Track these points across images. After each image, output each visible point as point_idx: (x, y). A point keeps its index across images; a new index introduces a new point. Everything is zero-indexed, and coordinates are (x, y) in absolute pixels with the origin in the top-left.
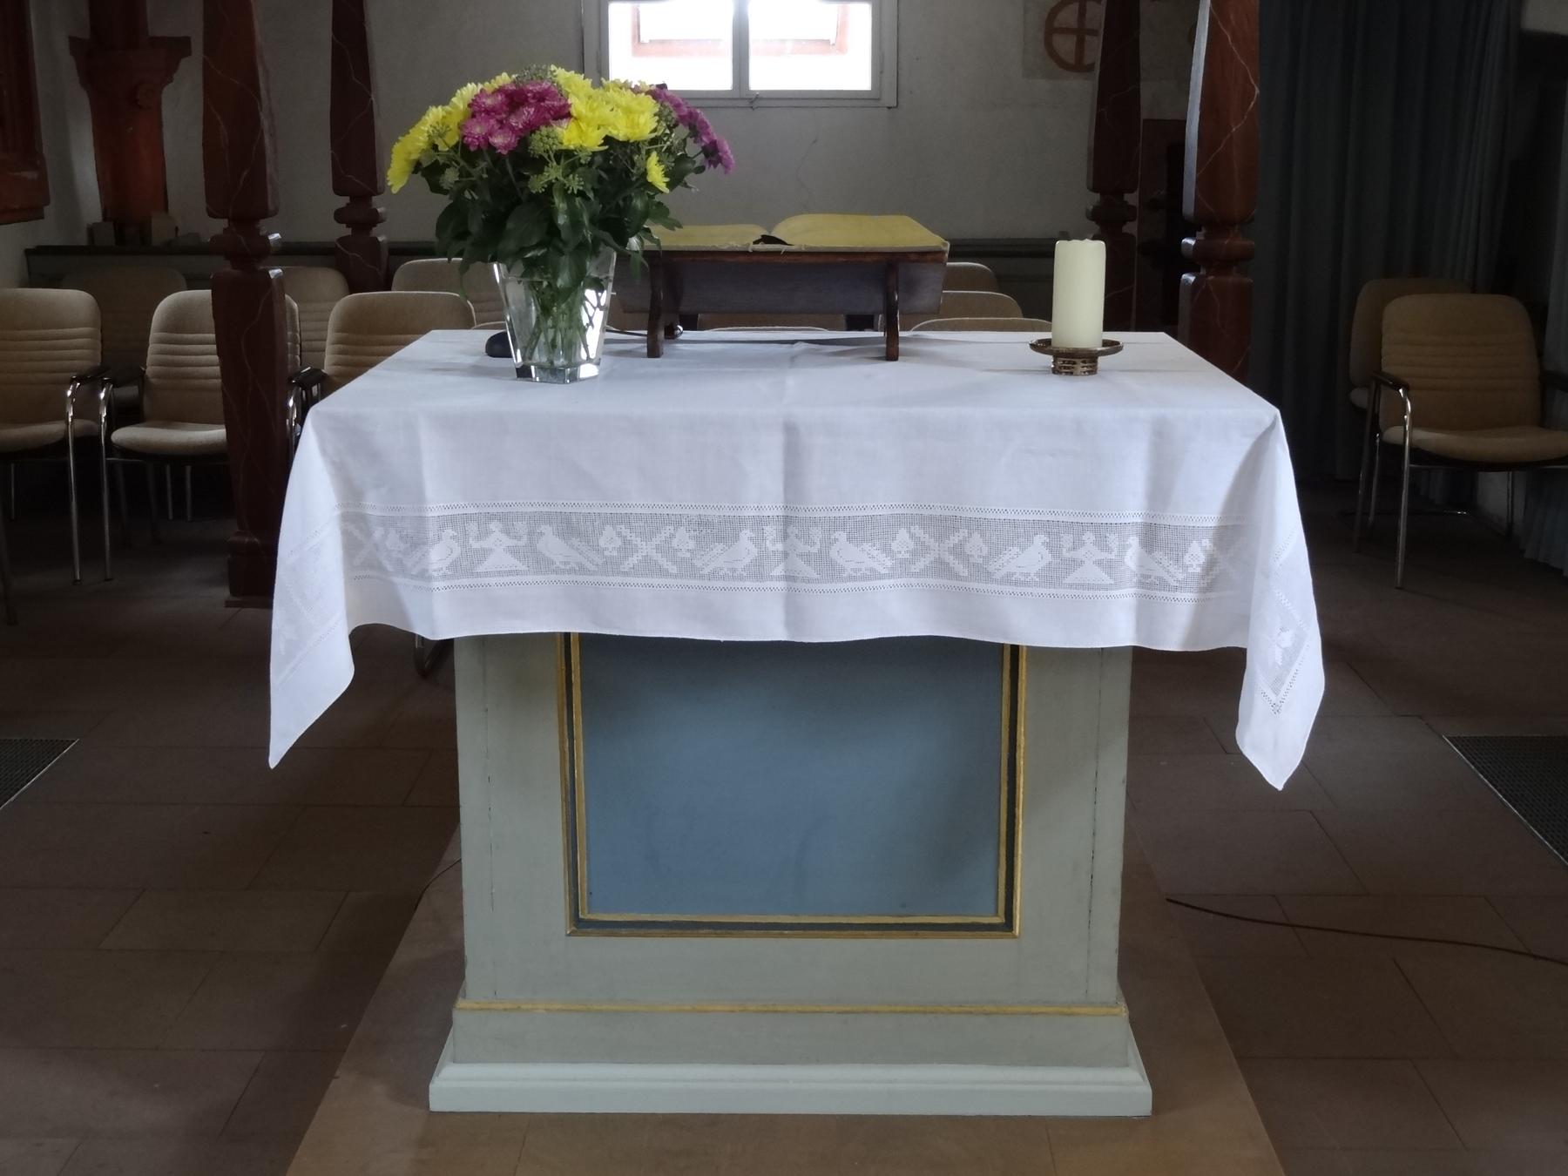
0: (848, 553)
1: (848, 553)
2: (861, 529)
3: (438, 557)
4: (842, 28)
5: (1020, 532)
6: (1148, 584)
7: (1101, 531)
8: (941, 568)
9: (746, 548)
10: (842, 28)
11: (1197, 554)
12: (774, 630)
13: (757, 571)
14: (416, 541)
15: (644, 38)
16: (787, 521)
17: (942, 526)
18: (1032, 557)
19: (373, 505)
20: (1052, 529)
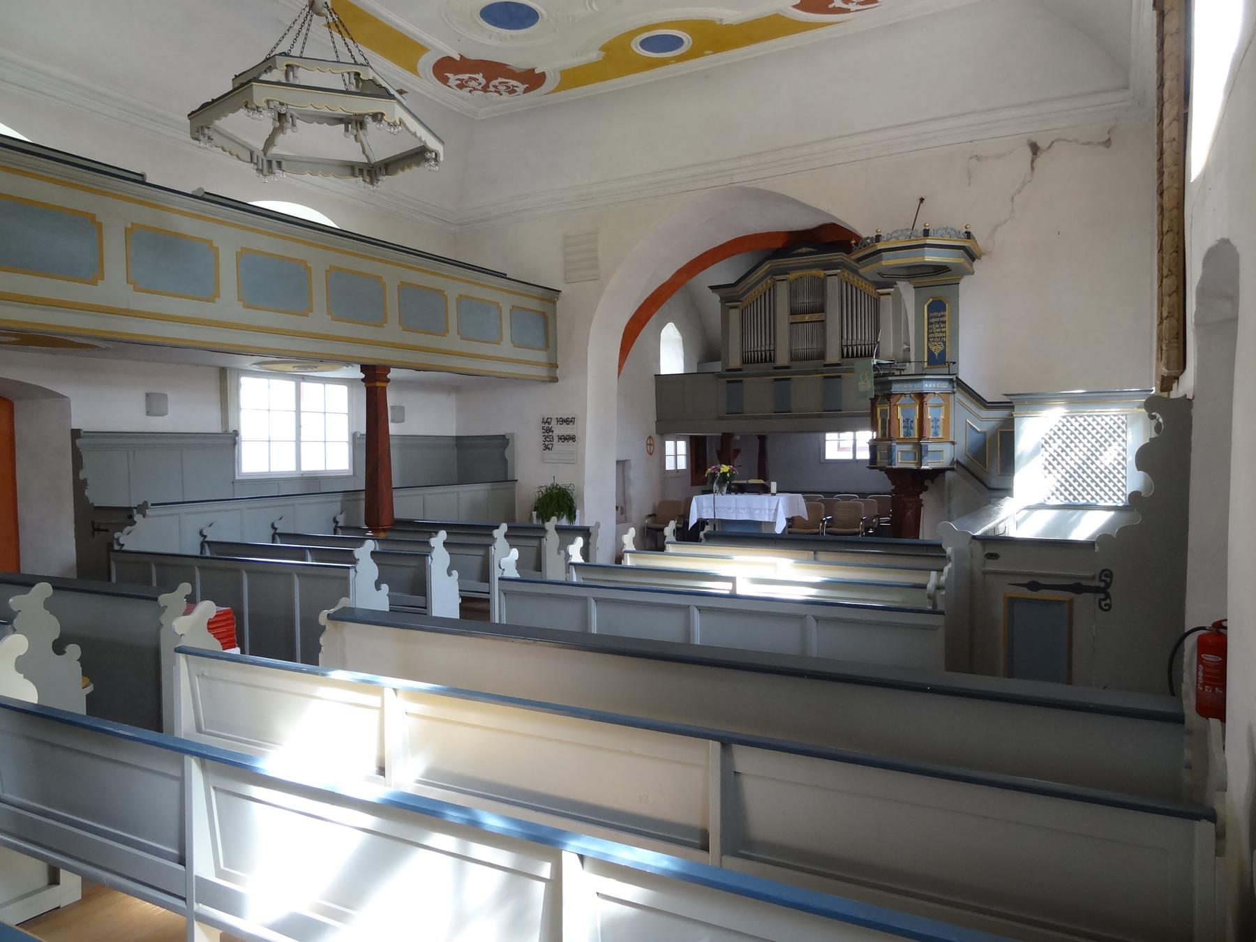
0: (741, 511)
1: (741, 511)
2: (742, 509)
3: (704, 510)
4: (844, 449)
5: (756, 509)
6: (769, 514)
7: (764, 509)
8: (750, 513)
9: (732, 511)
10: (844, 449)
11: (773, 512)
12: (734, 518)
13: (733, 512)
14: (702, 508)
15: (841, 447)
16: (736, 508)
17: (749, 508)
18: (758, 512)
19: (699, 505)
20: (760, 509)
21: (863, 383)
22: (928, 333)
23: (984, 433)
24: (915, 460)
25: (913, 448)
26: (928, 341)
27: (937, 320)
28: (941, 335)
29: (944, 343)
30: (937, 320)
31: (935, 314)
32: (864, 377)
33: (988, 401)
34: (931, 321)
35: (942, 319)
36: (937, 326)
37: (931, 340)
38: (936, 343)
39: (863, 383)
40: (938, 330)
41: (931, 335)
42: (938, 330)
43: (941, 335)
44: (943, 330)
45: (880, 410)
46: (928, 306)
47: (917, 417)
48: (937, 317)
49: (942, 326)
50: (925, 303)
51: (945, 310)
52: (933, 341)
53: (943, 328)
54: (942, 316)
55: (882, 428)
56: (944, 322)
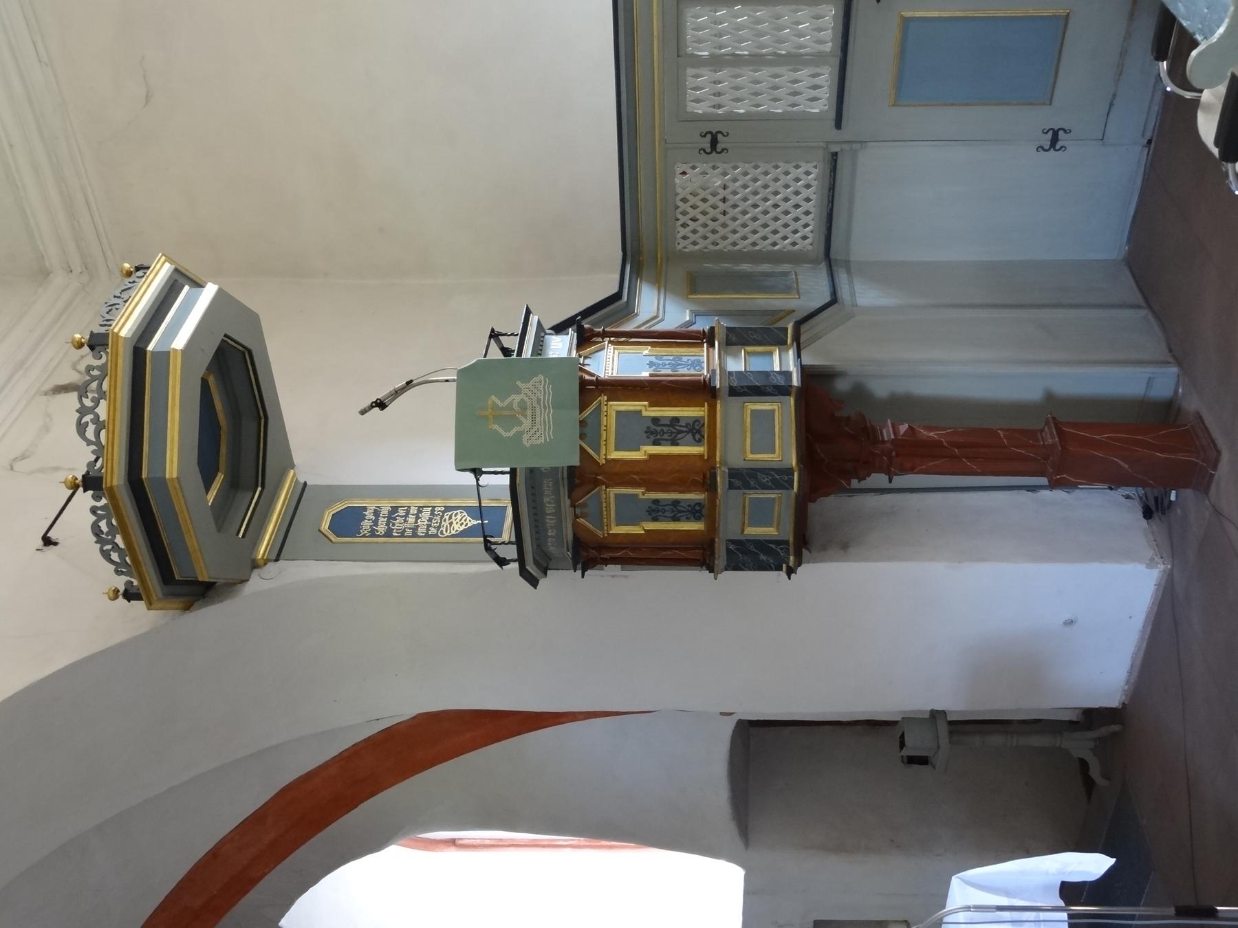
21: (527, 423)
22: (415, 535)
23: (696, 314)
24: (771, 354)
25: (736, 355)
26: (436, 536)
27: (382, 522)
28: (425, 515)
29: (448, 509)
30: (382, 522)
31: (366, 524)
32: (509, 418)
33: (615, 290)
34: (382, 528)
35: (385, 512)
36: (400, 520)
37: (433, 531)
38: (446, 524)
39: (527, 423)
40: (411, 519)
41: (421, 532)
42: (411, 519)
43: (425, 515)
44: (414, 510)
45: (617, 449)
46: (338, 536)
47: (647, 350)
48: (376, 523)
49: (401, 512)
50: (331, 541)
51: (365, 509)
52: (439, 528)
53: (408, 513)
54: (377, 513)
55: (674, 443)
56: (395, 509)
